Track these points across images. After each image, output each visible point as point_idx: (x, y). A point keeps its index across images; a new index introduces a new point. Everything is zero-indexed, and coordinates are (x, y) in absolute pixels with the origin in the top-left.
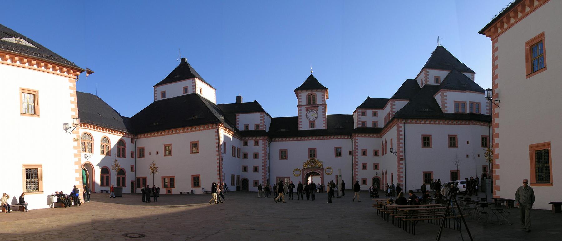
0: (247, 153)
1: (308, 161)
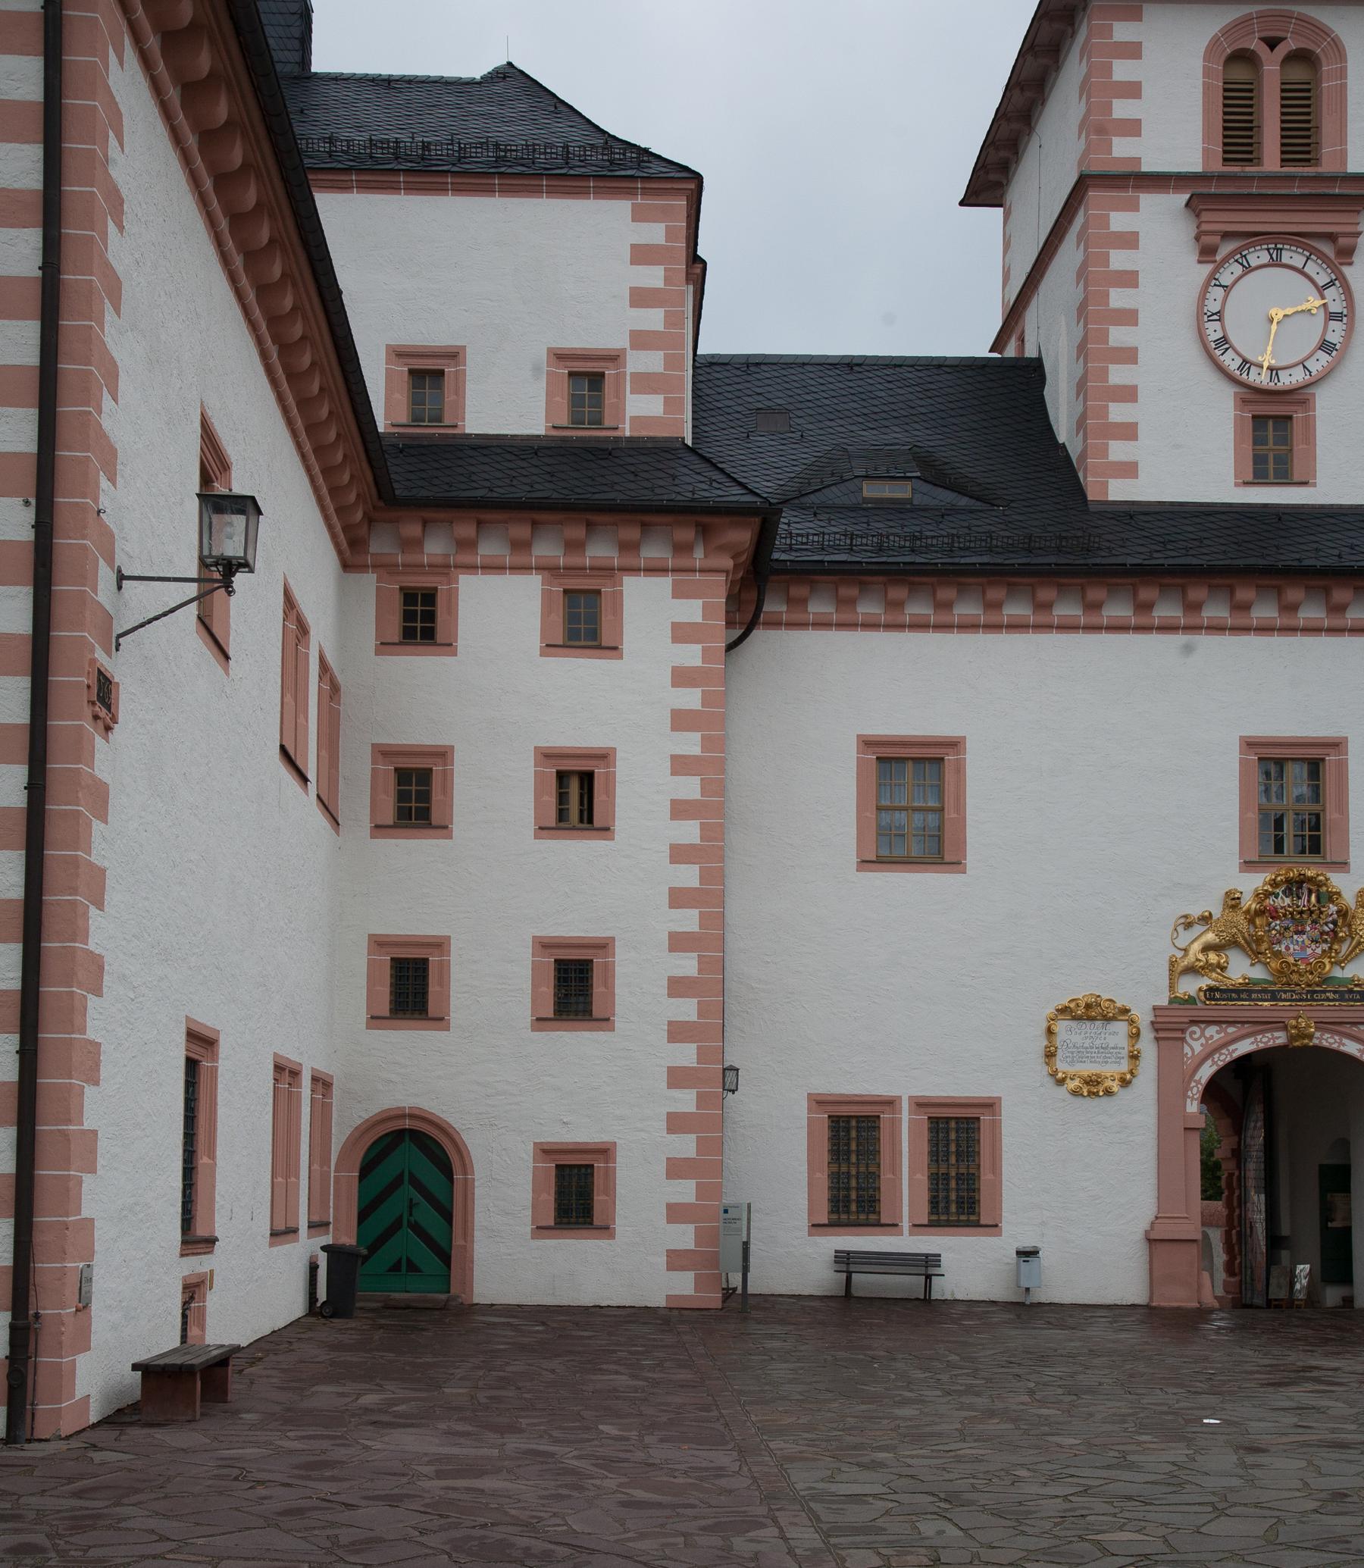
0: (443, 754)
1: (1232, 901)
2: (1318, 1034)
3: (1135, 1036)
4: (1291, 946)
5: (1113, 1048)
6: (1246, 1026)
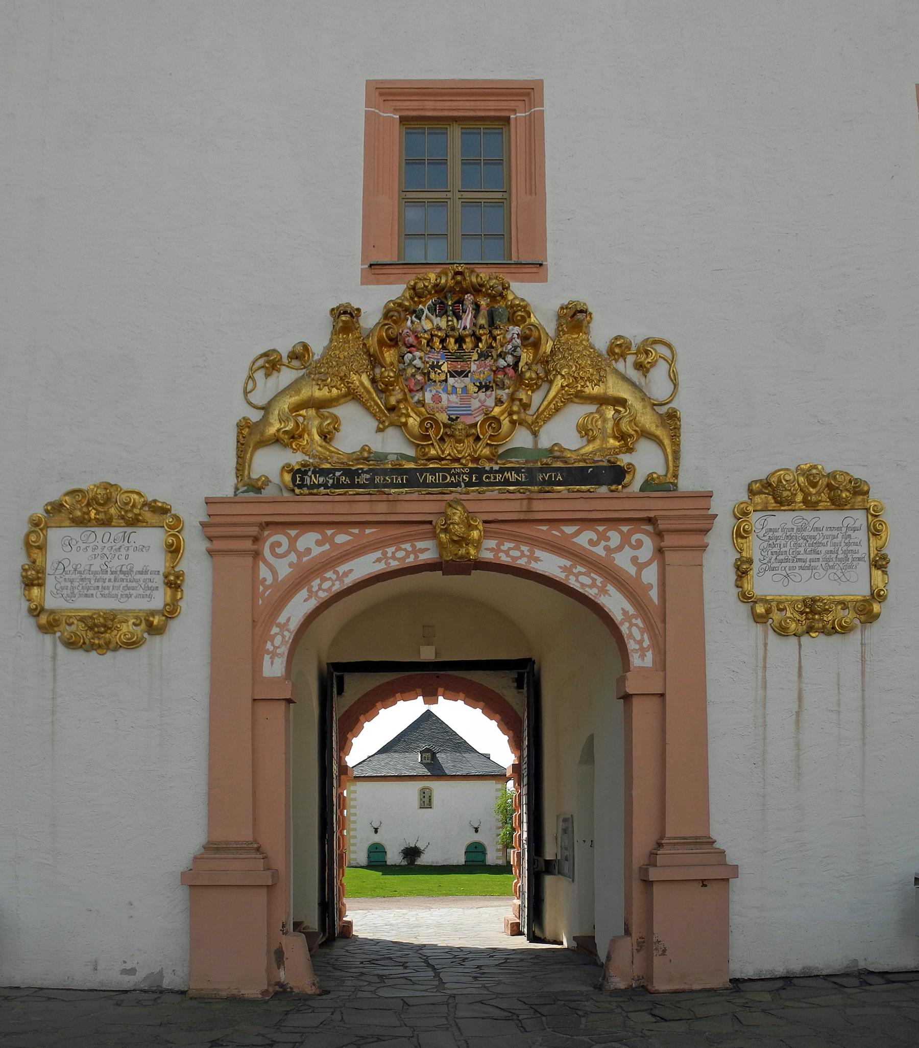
2: (491, 543)
3: (174, 550)
4: (444, 396)
5: (141, 573)
6: (368, 531)
